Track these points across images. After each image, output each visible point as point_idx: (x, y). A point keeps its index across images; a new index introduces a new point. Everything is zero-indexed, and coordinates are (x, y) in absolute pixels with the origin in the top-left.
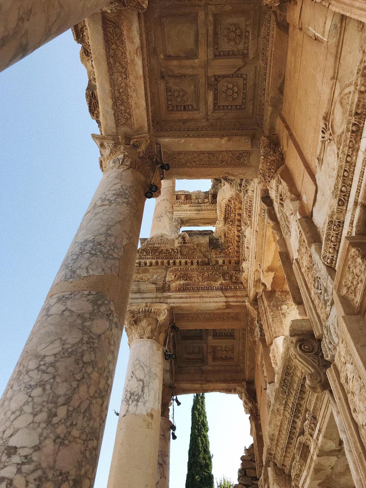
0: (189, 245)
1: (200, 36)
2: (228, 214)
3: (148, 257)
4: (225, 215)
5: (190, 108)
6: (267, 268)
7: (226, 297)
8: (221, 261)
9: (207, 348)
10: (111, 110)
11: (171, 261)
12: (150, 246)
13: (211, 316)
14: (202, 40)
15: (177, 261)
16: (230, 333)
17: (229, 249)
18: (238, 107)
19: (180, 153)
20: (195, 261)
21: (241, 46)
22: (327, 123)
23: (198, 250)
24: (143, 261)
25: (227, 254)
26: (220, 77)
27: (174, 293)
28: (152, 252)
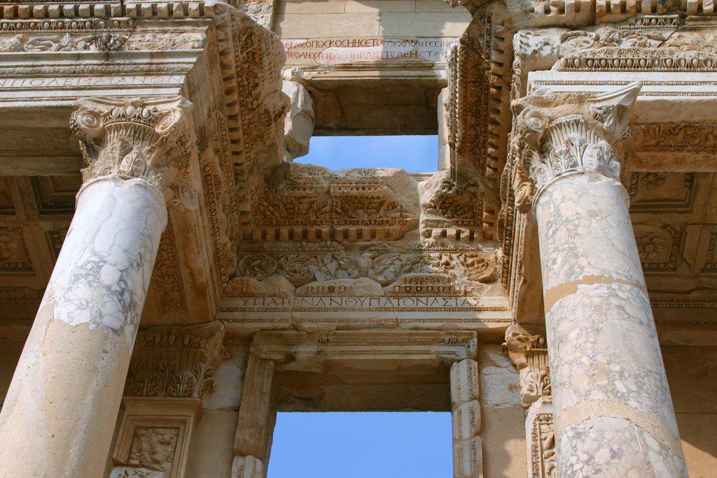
8: (247, 207)
10: (681, 119)
17: (271, 209)
28: (247, 53)
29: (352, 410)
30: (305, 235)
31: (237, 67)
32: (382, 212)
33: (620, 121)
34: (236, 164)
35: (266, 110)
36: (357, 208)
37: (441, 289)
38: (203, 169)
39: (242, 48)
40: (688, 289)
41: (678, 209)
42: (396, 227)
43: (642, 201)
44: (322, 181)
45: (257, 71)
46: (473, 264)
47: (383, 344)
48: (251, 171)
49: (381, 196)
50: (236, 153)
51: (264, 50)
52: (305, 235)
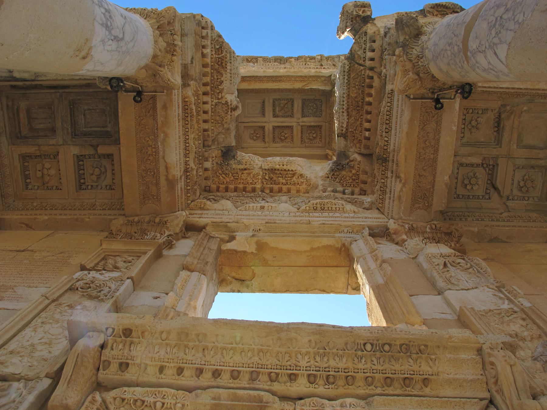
0: (229, 117)
2: (280, 174)
3: (214, 52)
4: (278, 170)
6: (264, 241)
7: (181, 178)
8: (208, 165)
9: (53, 145)
12: (228, 55)
13: (150, 156)
16: (85, 183)
17: (224, 176)
19: (439, 123)
21: (516, 192)
23: (220, 129)
25: (216, 173)
26: (489, 170)
28: (219, 58)
29: (275, 291)
30: (244, 189)
32: (294, 179)
34: (205, 130)
35: (226, 101)
36: (279, 177)
37: (338, 209)
42: (304, 186)
44: (257, 161)
45: (223, 72)
47: (300, 232)
49: (294, 169)
50: (205, 121)
51: (228, 58)
52: (244, 189)
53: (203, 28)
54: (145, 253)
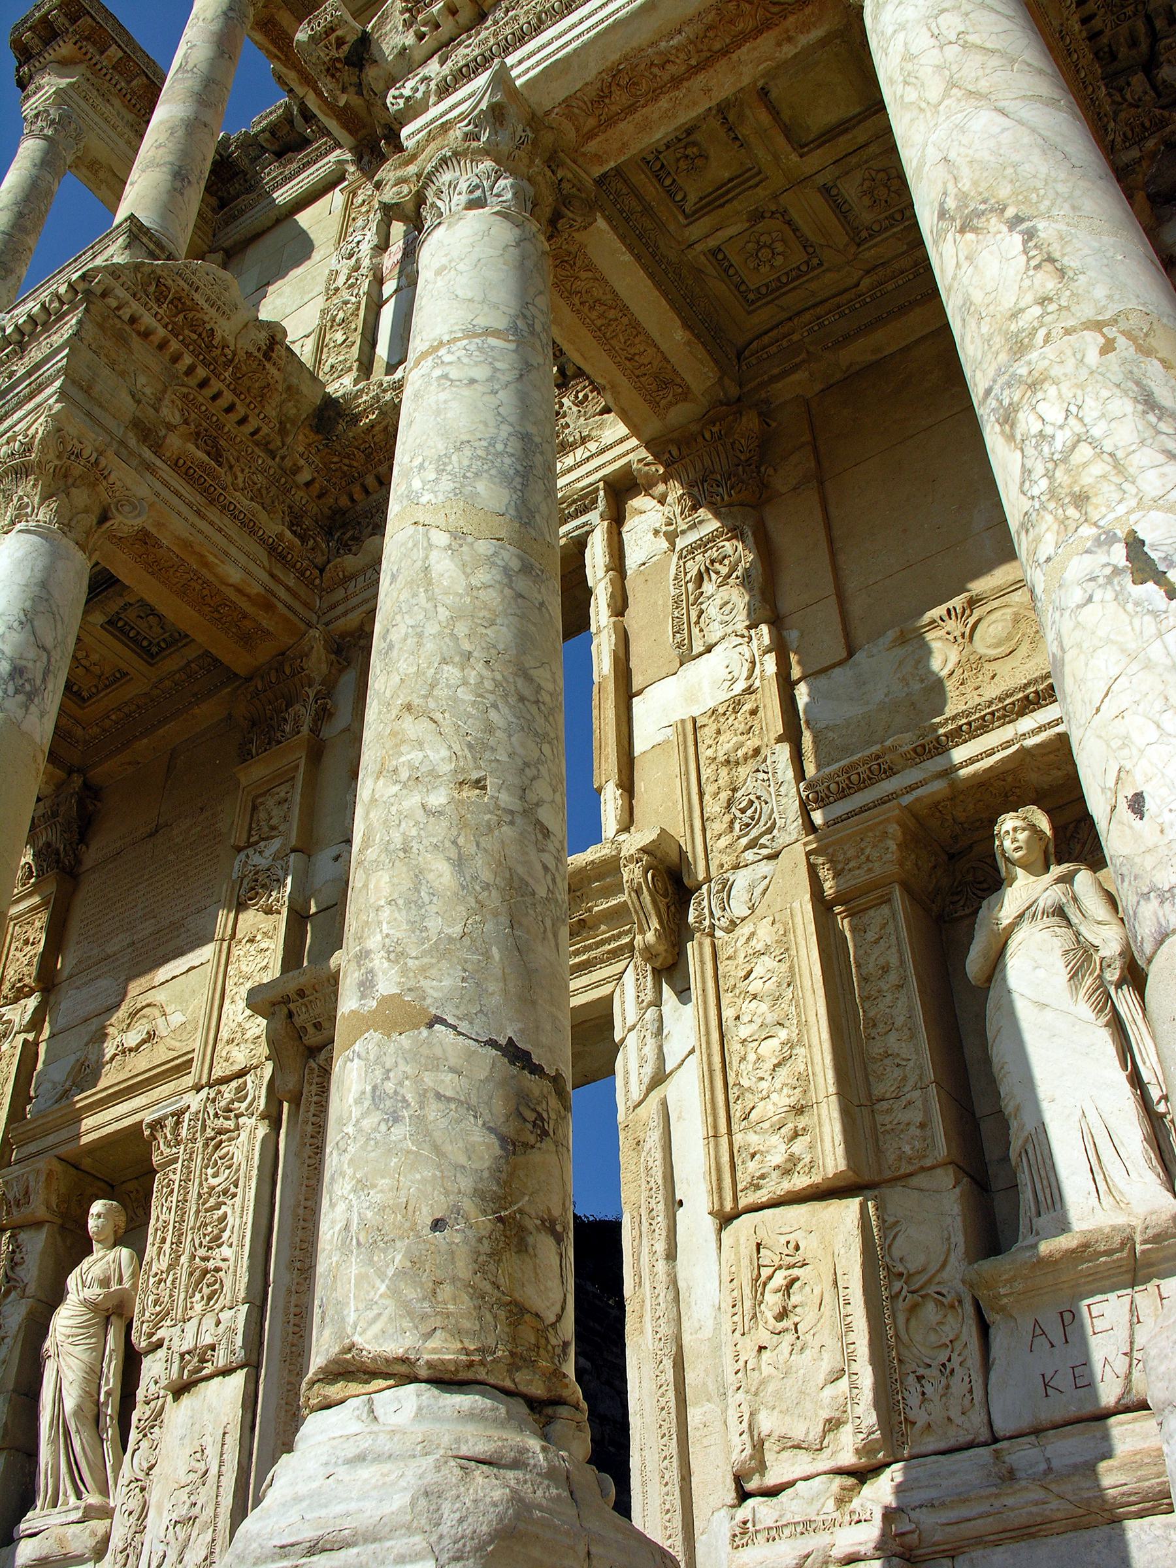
1: (850, 136)
3: (155, 307)
5: (678, 198)
8: (305, 476)
10: (594, 72)
11: (201, 372)
14: (844, 143)
15: (216, 385)
17: (346, 461)
18: (743, 288)
19: (590, 267)
20: (254, 423)
22: (968, 612)
24: (135, 307)
27: (164, 466)
28: (171, 302)
31: (165, 326)
33: (501, 124)
34: (253, 434)
38: (175, 465)
39: (158, 300)
40: (855, 280)
41: (751, 183)
43: (701, 199)
45: (199, 315)
46: (586, 397)
48: (283, 431)
50: (243, 421)
53: (104, 295)
54: (298, 766)
